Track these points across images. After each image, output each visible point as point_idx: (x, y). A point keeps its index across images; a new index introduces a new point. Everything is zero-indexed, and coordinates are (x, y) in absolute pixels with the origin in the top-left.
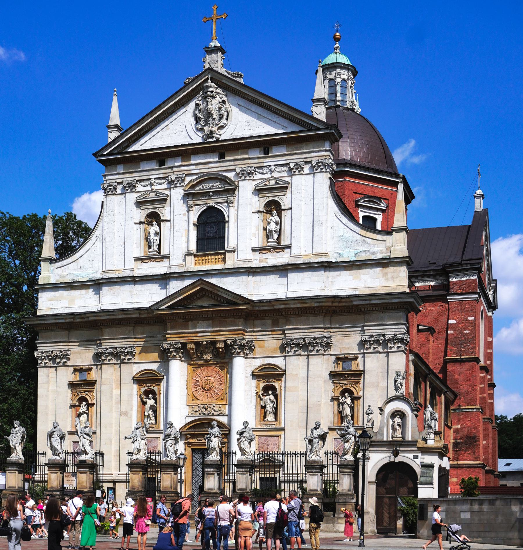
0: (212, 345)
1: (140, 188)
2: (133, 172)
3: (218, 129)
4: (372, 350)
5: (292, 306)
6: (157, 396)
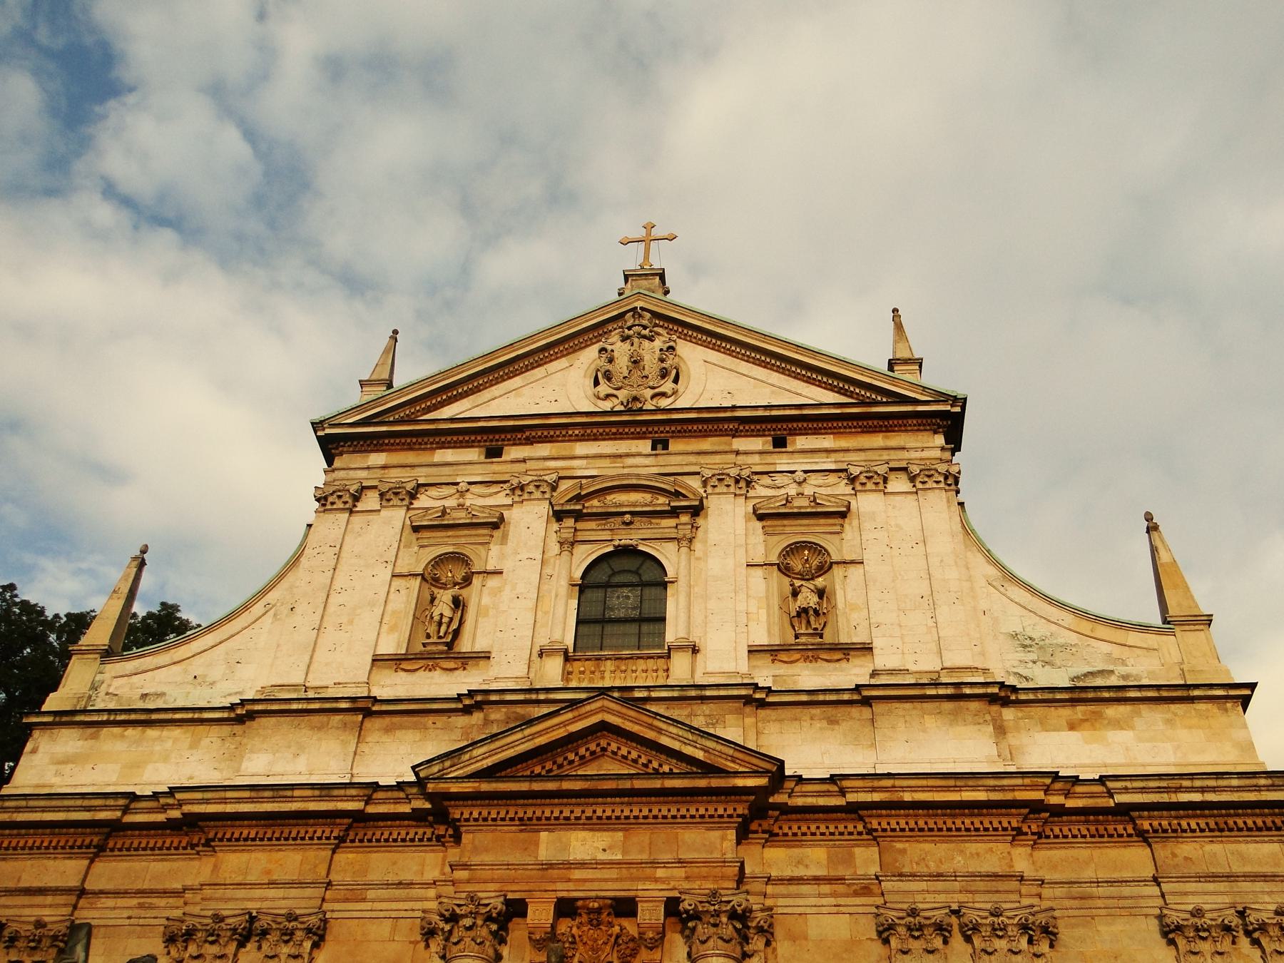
1: (423, 501)
2: (412, 466)
3: (652, 397)
5: (907, 797)
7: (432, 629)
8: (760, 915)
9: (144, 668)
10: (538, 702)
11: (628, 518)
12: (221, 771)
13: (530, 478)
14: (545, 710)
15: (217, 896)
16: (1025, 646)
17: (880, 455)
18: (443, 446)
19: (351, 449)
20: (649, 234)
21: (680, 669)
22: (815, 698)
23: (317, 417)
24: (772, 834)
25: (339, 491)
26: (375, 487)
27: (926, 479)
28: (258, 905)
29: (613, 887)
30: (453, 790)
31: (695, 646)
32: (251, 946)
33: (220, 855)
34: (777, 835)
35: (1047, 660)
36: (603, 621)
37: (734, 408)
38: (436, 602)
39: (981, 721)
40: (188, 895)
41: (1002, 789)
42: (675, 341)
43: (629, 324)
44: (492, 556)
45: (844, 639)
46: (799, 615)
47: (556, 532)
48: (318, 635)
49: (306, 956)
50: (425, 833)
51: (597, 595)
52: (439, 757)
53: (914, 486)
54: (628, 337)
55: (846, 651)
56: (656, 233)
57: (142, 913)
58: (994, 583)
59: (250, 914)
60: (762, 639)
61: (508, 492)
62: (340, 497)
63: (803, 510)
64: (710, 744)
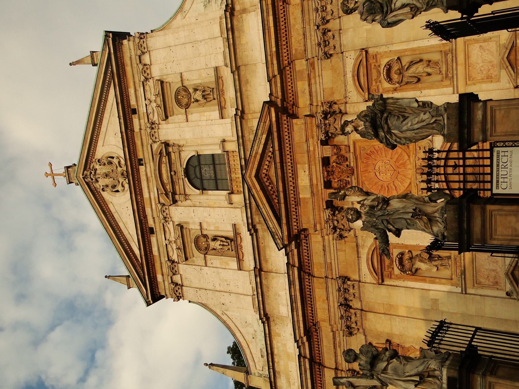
1: (175, 257)
2: (161, 263)
3: (121, 167)
5: (274, 49)
7: (226, 248)
8: (325, 107)
9: (251, 358)
10: (250, 203)
11: (173, 173)
12: (288, 323)
13: (161, 215)
14: (253, 200)
15: (334, 319)
17: (135, 68)
18: (151, 252)
20: (50, 175)
21: (232, 146)
22: (238, 90)
23: (144, 304)
24: (293, 104)
25: (174, 291)
26: (171, 278)
27: (143, 47)
28: (336, 303)
29: (318, 167)
30: (286, 234)
31: (222, 141)
33: (319, 320)
34: (294, 102)
36: (216, 179)
37: (121, 132)
38: (215, 248)
39: (241, 19)
40: (334, 330)
41: (267, 9)
42: (96, 160)
43: (90, 180)
44: (194, 227)
45: (213, 79)
46: (205, 99)
47: (182, 202)
48: (232, 293)
49: (353, 283)
50: (304, 243)
51: (206, 183)
52: (274, 241)
53: (146, 52)
55: (218, 78)
56: (49, 172)
57: (342, 345)
58: (184, 16)
59: (339, 306)
60: (216, 114)
61: (167, 223)
62: (177, 291)
63: (162, 100)
64: (260, 132)
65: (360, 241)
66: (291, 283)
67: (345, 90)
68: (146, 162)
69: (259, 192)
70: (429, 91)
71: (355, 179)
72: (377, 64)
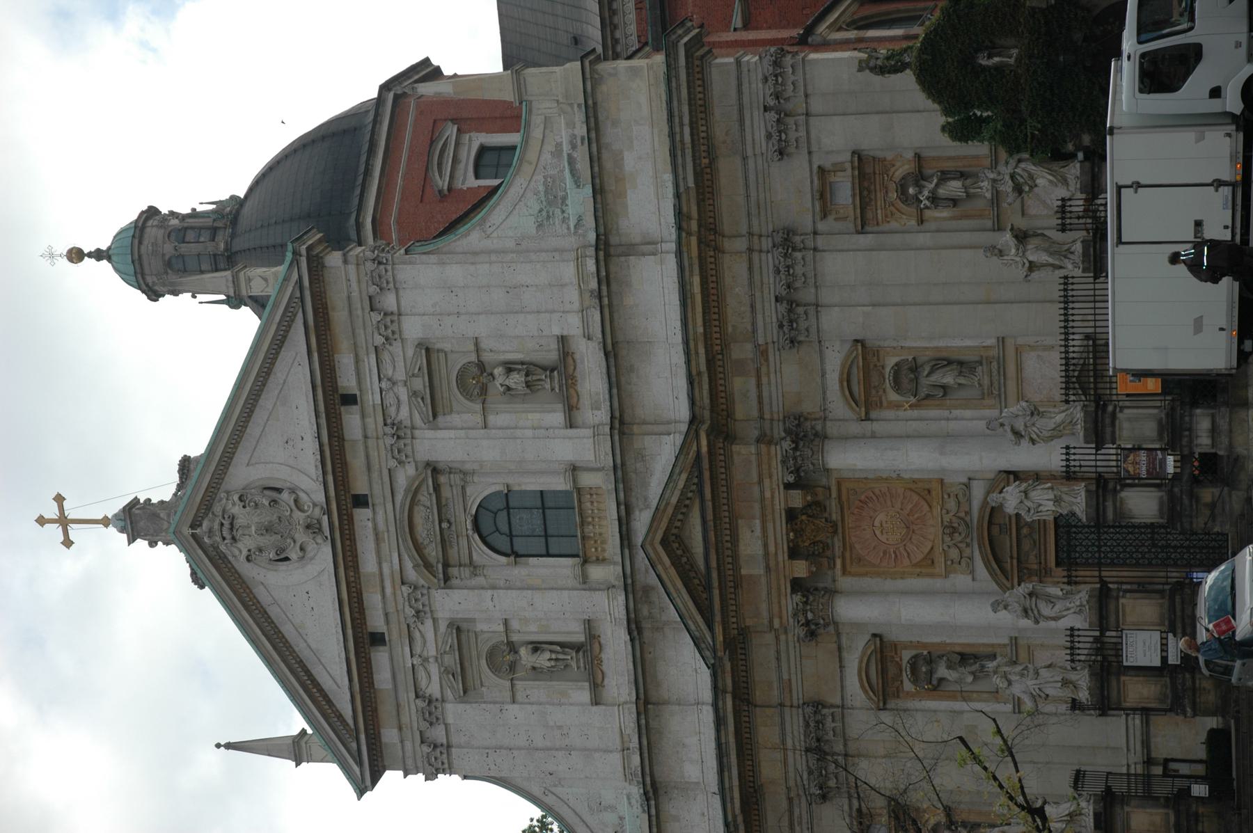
0: (797, 518)
2: (398, 705)
4: (802, 133)
5: (701, 330)
6: (925, 653)
7: (561, 665)
8: (787, 425)
13: (407, 607)
16: (548, 217)
19: (380, 759)
24: (728, 416)
30: (721, 638)
32: (826, 748)
35: (560, 201)
40: (792, 795)
41: (691, 265)
43: (218, 539)
48: (574, 750)
49: (832, 710)
52: (700, 653)
54: (234, 538)
56: (52, 511)
57: (804, 821)
60: (558, 418)
63: (427, 384)
64: (677, 470)
65: (844, 640)
66: (719, 722)
67: (824, 399)
68: (377, 501)
69: (670, 571)
70: (963, 411)
71: (839, 540)
72: (878, 364)
